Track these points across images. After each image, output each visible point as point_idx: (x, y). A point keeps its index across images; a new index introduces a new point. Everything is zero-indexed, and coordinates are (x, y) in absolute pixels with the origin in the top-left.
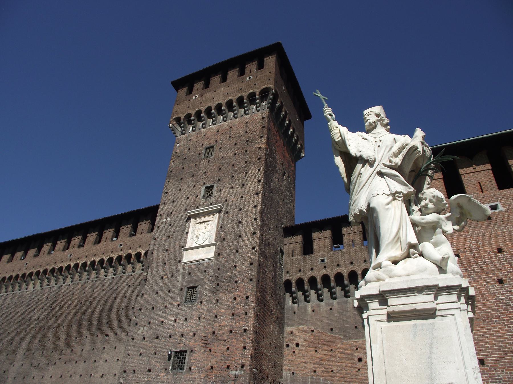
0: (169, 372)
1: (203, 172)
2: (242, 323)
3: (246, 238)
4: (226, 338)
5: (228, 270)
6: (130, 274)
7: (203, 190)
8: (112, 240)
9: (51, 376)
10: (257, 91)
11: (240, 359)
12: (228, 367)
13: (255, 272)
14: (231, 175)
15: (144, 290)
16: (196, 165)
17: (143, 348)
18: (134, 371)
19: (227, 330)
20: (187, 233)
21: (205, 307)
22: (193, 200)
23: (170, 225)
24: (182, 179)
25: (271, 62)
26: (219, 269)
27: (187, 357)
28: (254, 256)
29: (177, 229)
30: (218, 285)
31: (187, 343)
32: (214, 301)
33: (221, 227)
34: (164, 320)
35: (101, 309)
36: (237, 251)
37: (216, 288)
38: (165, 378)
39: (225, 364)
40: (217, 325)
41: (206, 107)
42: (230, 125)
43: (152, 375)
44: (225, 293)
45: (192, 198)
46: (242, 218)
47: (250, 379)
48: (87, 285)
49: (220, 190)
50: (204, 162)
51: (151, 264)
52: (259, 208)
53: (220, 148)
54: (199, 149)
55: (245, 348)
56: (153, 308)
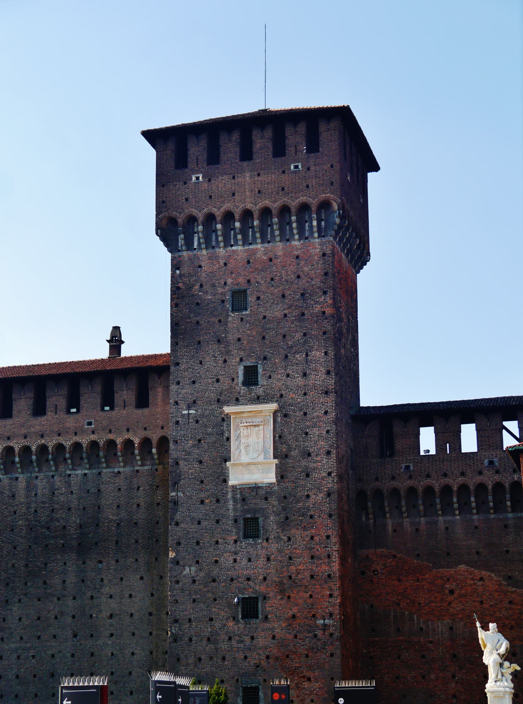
0: (238, 621)
1: (236, 336)
2: (324, 568)
3: (319, 458)
4: (307, 584)
5: (298, 502)
6: (116, 470)
7: (241, 371)
8: (69, 412)
9: (20, 619)
10: (314, 203)
11: (327, 608)
12: (314, 616)
13: (334, 506)
14: (283, 352)
15: (178, 517)
16: (220, 321)
17: (196, 593)
18: (190, 620)
19: (308, 574)
20: (228, 439)
21: (274, 547)
22: (226, 387)
23: (197, 422)
24: (199, 343)
25: (330, 136)
26: (285, 497)
27: (260, 604)
28: (331, 483)
29: (210, 430)
30: (287, 518)
31: (257, 588)
32: (285, 538)
33: (279, 439)
34: (218, 559)
35: (78, 521)
36: (308, 475)
37: (285, 523)
38: (235, 626)
39: (309, 612)
40: (293, 568)
41: (222, 210)
42: (271, 255)
43: (217, 625)
44: (298, 529)
45: (225, 383)
46: (308, 427)
47: (341, 629)
48: (38, 482)
49: (270, 377)
50: (233, 317)
51: (180, 480)
52: (332, 415)
53: (258, 298)
54: (220, 290)
55: (331, 596)
56: (198, 543)
